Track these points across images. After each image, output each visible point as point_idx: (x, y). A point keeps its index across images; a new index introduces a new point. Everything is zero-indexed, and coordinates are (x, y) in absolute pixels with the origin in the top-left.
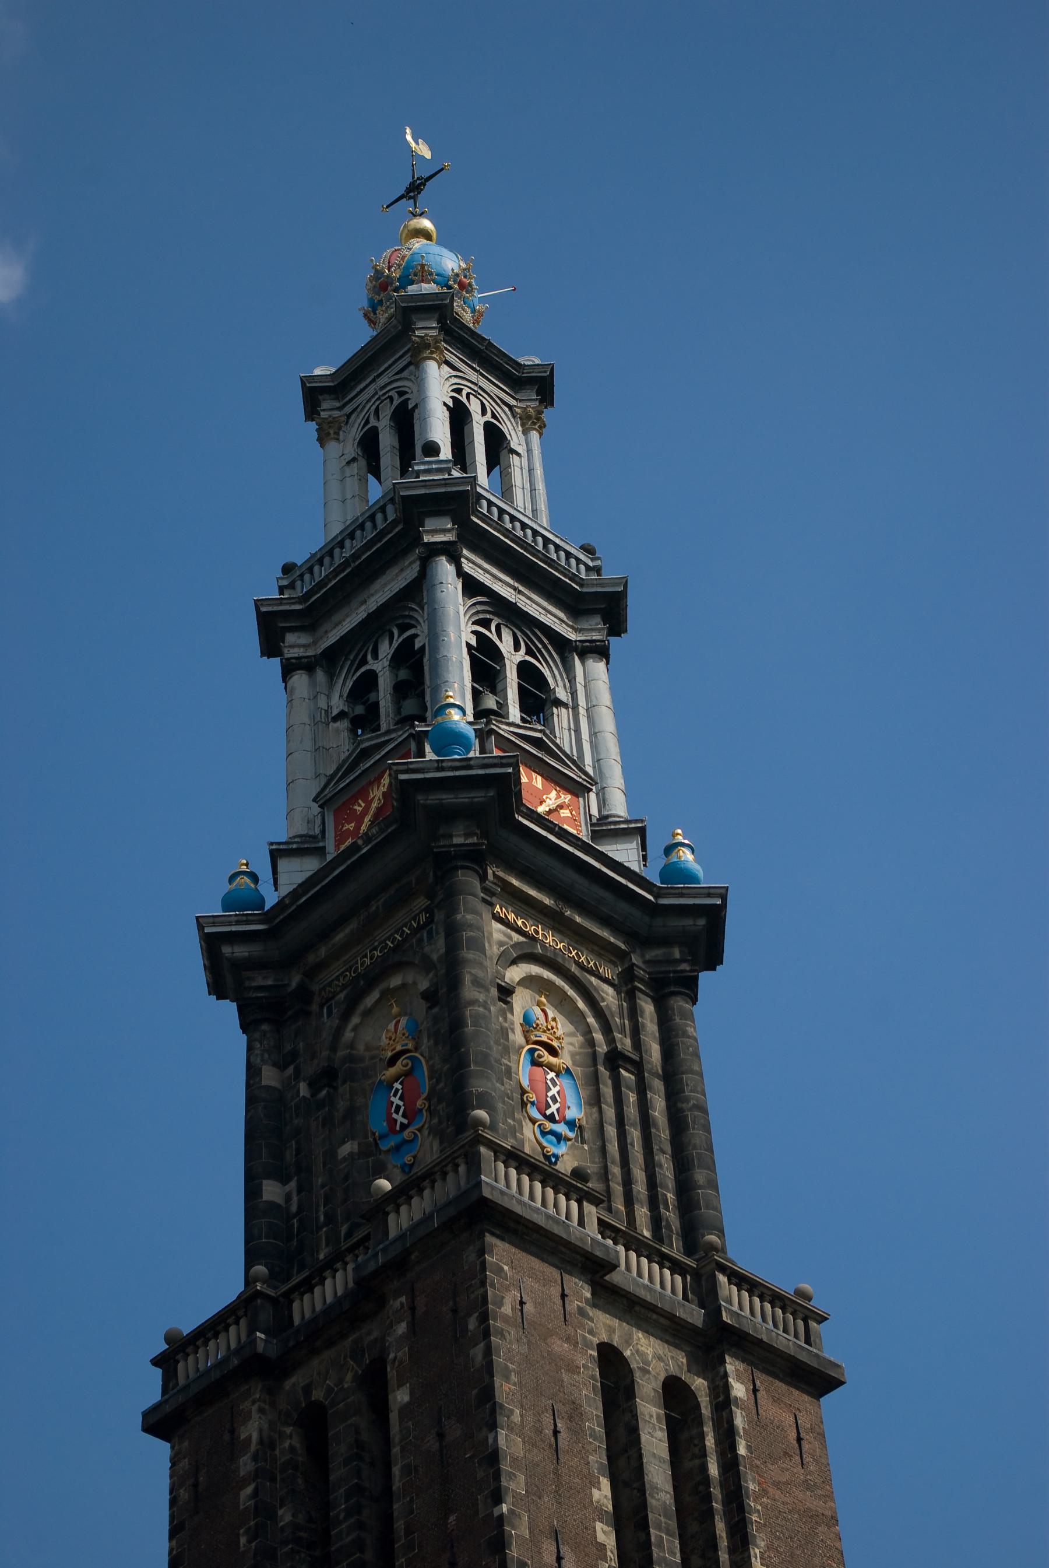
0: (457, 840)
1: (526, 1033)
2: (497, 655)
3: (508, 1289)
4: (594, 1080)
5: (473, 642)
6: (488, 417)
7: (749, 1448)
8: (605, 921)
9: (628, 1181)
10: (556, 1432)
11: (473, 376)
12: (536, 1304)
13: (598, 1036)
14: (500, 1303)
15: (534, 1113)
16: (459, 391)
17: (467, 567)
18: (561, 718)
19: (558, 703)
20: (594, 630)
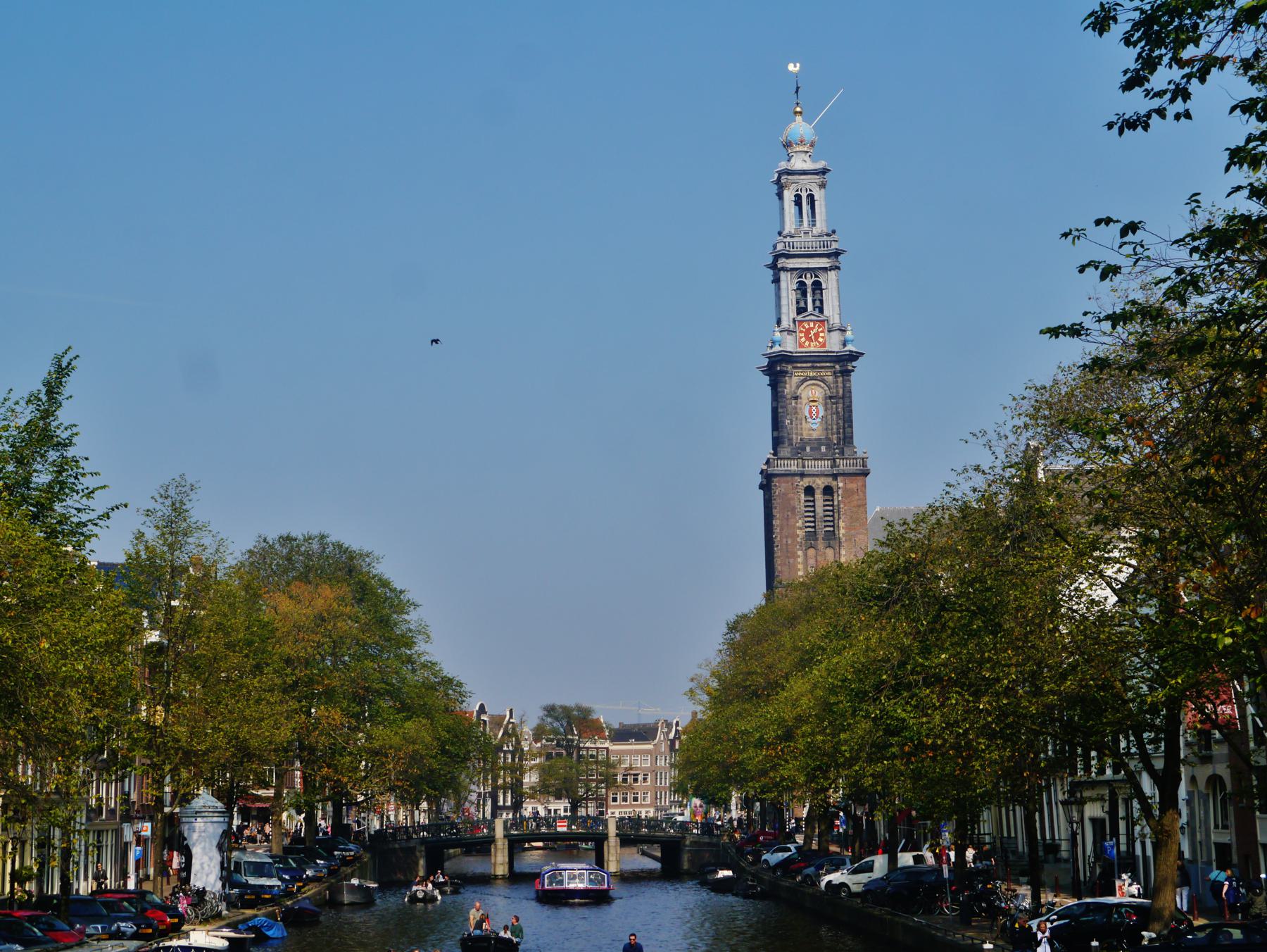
4: (826, 404)
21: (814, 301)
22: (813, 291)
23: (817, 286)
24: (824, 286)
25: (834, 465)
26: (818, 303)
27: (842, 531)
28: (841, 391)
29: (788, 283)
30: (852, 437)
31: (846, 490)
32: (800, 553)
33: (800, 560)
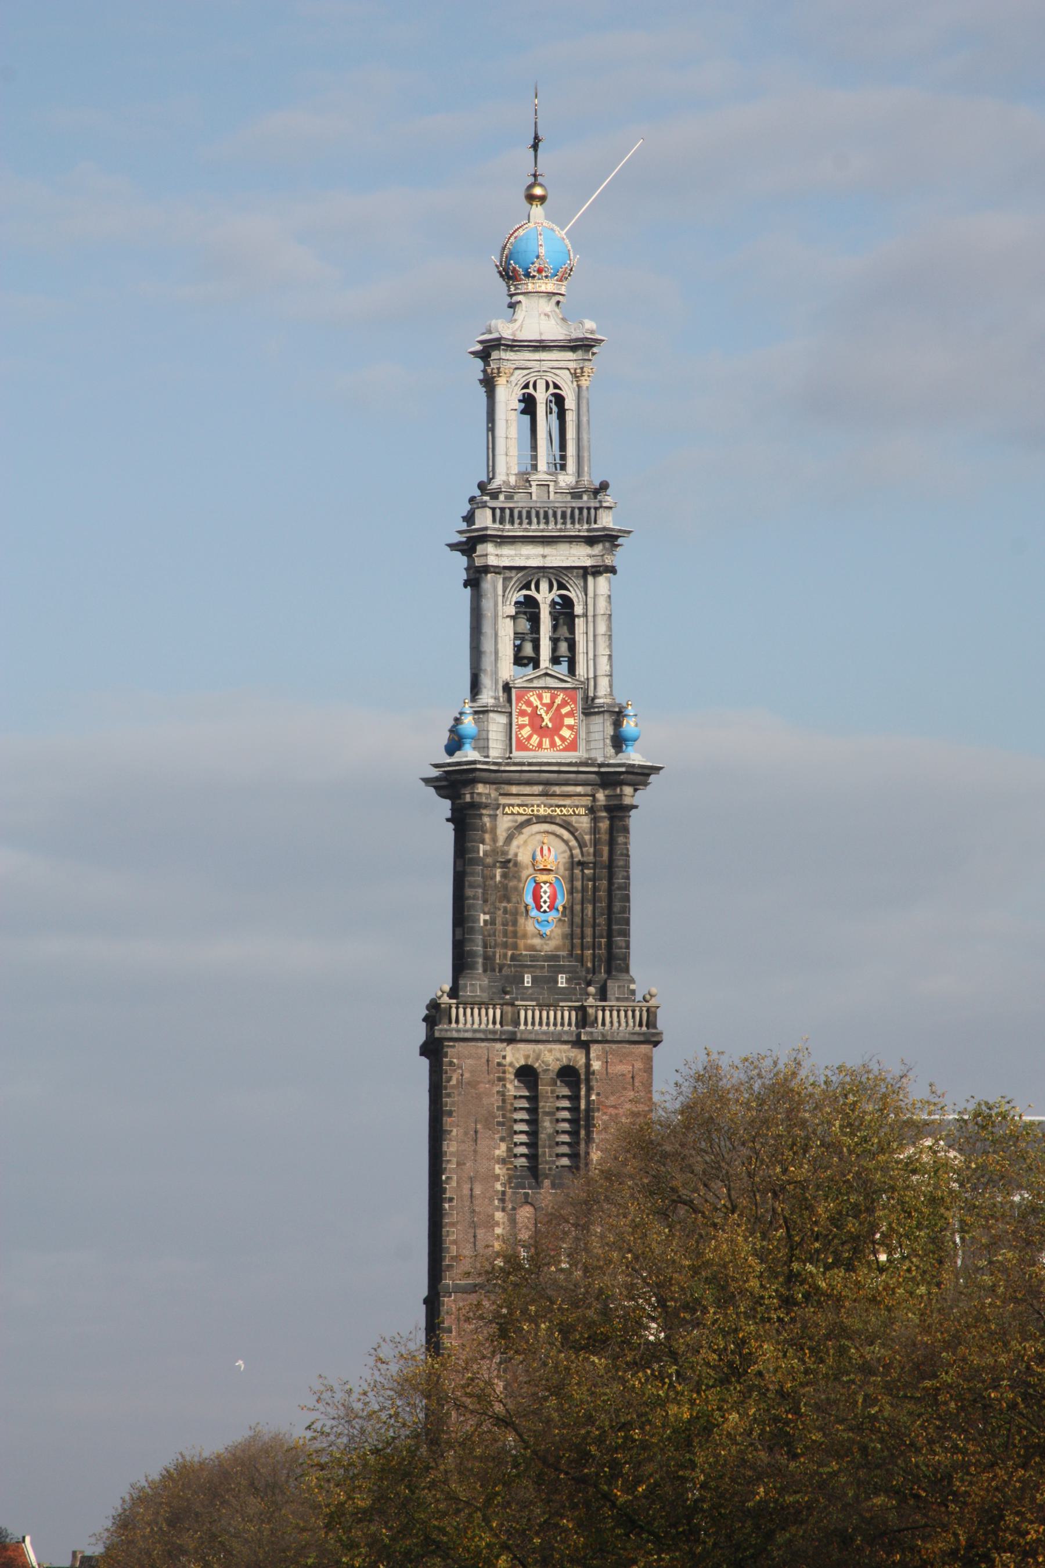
3: (455, 1070)
4: (572, 879)
6: (552, 390)
10: (476, 1132)
12: (471, 1072)
13: (577, 852)
14: (449, 1080)
19: (578, 616)
21: (555, 641)
22: (555, 617)
23: (564, 613)
24: (578, 610)
25: (584, 1019)
26: (563, 647)
29: (502, 603)
30: (626, 958)
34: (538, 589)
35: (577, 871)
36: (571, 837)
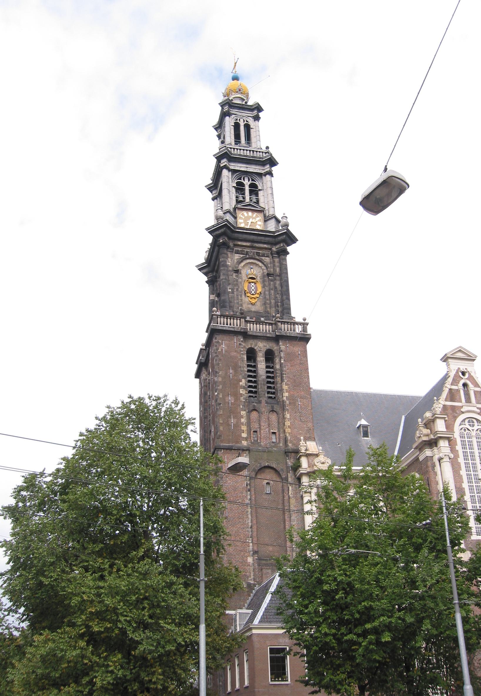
0: (221, 241)
1: (247, 276)
2: (243, 185)
4: (264, 281)
5: (235, 185)
6: (245, 122)
7: (285, 360)
8: (264, 243)
9: (271, 303)
11: (240, 114)
15: (249, 295)
16: (237, 120)
17: (232, 168)
18: (261, 193)
19: (260, 190)
20: (267, 168)
24: (260, 188)
27: (286, 394)
28: (278, 270)
30: (289, 309)
31: (288, 354)
32: (243, 413)
33: (243, 420)
34: (244, 180)
35: (266, 279)
36: (263, 265)
